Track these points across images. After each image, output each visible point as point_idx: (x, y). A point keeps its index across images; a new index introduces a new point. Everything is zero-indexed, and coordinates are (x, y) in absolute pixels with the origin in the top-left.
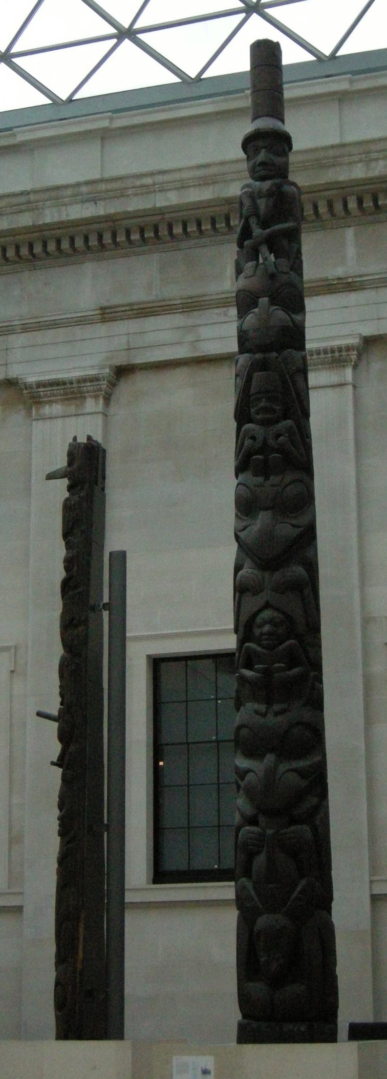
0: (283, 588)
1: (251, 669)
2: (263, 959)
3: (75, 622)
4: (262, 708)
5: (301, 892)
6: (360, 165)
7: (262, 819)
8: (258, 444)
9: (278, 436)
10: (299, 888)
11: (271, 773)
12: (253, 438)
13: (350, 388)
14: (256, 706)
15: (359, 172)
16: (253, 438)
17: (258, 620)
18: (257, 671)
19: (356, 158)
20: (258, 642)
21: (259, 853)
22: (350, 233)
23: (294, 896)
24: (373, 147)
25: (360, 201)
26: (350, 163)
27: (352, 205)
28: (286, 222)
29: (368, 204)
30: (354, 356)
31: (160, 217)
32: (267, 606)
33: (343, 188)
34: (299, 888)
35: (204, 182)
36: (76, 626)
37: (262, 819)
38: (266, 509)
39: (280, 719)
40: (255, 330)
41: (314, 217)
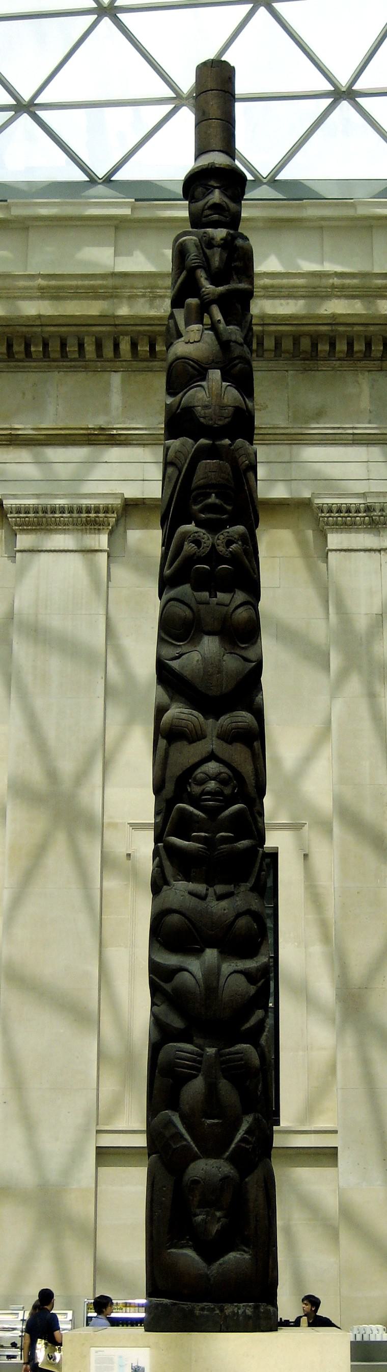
0: (230, 737)
2: (200, 1218)
4: (200, 888)
5: (246, 1132)
6: (142, 300)
8: (205, 550)
9: (229, 543)
10: (244, 1127)
11: (212, 975)
12: (197, 542)
13: (106, 554)
14: (192, 886)
16: (197, 542)
17: (199, 773)
18: (197, 840)
19: (139, 292)
20: (195, 801)
21: (195, 1076)
22: (116, 379)
23: (238, 1137)
25: (134, 345)
27: (125, 346)
28: (240, 282)
29: (144, 348)
32: (212, 756)
33: (116, 325)
34: (244, 1127)
38: (209, 633)
39: (224, 903)
40: (206, 407)
41: (76, 356)
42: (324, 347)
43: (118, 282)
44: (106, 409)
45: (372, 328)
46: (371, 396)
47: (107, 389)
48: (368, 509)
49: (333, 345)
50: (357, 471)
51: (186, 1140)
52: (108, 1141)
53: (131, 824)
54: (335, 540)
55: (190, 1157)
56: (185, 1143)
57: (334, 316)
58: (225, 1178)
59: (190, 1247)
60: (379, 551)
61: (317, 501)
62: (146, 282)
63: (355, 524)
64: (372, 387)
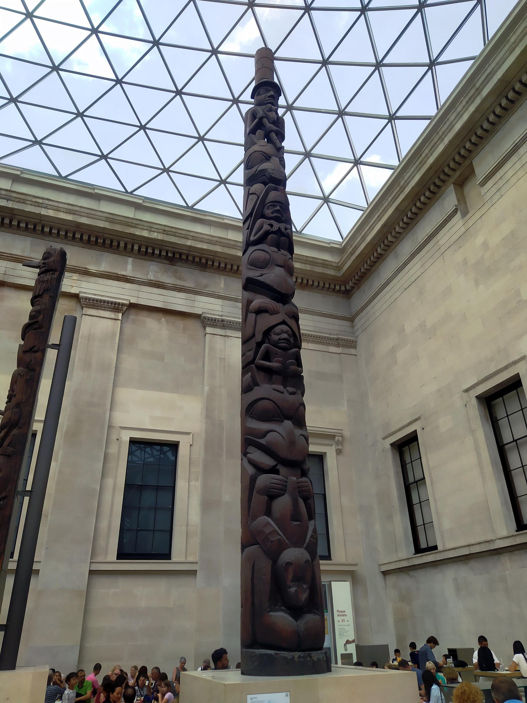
1: (270, 362)
2: (293, 590)
3: (35, 349)
4: (281, 388)
7: (282, 469)
8: (275, 228)
12: (271, 226)
14: (274, 386)
15: (145, 234)
16: (271, 226)
17: (277, 329)
19: (145, 228)
21: (283, 495)
22: (130, 260)
24: (154, 226)
26: (142, 229)
27: (136, 247)
30: (125, 308)
31: (39, 221)
32: (284, 323)
35: (70, 212)
36: (36, 352)
37: (280, 468)
39: (292, 397)
42: (210, 263)
43: (138, 222)
44: (126, 270)
45: (227, 260)
47: (126, 263)
48: (223, 321)
50: (219, 308)
51: (280, 535)
52: (95, 567)
53: (120, 427)
54: (209, 330)
55: (282, 547)
56: (280, 537)
57: (216, 252)
58: (307, 561)
59: (282, 611)
61: (204, 315)
62: (149, 225)
63: (217, 325)
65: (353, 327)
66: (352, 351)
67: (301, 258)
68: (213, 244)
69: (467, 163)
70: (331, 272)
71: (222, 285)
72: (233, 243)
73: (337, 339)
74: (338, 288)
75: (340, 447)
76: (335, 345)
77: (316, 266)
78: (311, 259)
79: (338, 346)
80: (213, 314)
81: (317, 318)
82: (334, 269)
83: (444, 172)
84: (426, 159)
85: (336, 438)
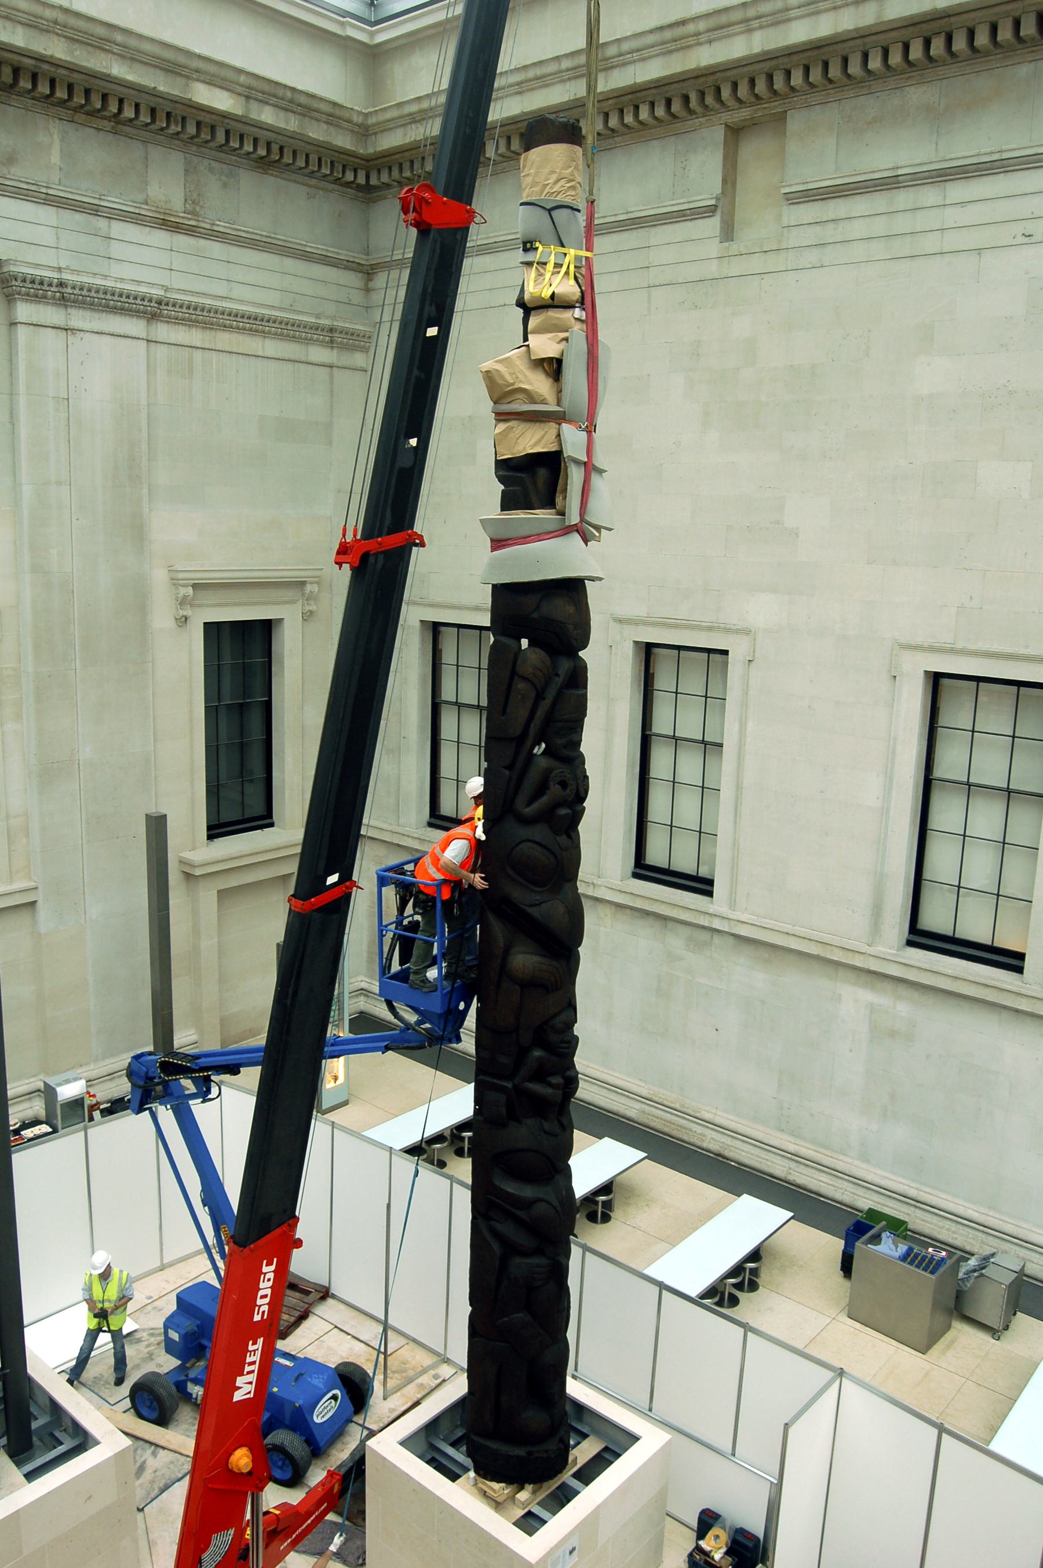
45: (75, 75)
46: (61, 151)
48: (61, 284)
49: (35, 85)
50: (47, 236)
54: (24, 311)
60: (66, 330)
63: (45, 297)
64: (62, 140)
65: (367, 290)
66: (359, 359)
67: (281, 92)
68: (42, 30)
69: (776, 106)
70: (343, 141)
71: (55, 158)
72: (101, 31)
73: (331, 330)
74: (349, 176)
75: (313, 608)
76: (322, 343)
77: (312, 118)
78: (303, 100)
79: (331, 344)
80: (37, 266)
81: (291, 264)
82: (352, 131)
83: (718, 90)
84: (691, 41)
85: (309, 588)
